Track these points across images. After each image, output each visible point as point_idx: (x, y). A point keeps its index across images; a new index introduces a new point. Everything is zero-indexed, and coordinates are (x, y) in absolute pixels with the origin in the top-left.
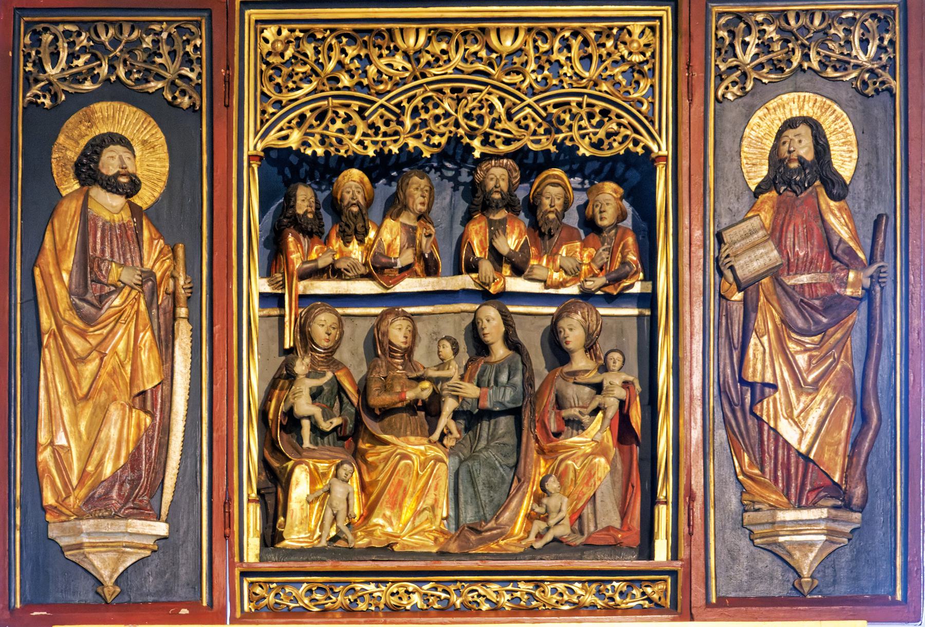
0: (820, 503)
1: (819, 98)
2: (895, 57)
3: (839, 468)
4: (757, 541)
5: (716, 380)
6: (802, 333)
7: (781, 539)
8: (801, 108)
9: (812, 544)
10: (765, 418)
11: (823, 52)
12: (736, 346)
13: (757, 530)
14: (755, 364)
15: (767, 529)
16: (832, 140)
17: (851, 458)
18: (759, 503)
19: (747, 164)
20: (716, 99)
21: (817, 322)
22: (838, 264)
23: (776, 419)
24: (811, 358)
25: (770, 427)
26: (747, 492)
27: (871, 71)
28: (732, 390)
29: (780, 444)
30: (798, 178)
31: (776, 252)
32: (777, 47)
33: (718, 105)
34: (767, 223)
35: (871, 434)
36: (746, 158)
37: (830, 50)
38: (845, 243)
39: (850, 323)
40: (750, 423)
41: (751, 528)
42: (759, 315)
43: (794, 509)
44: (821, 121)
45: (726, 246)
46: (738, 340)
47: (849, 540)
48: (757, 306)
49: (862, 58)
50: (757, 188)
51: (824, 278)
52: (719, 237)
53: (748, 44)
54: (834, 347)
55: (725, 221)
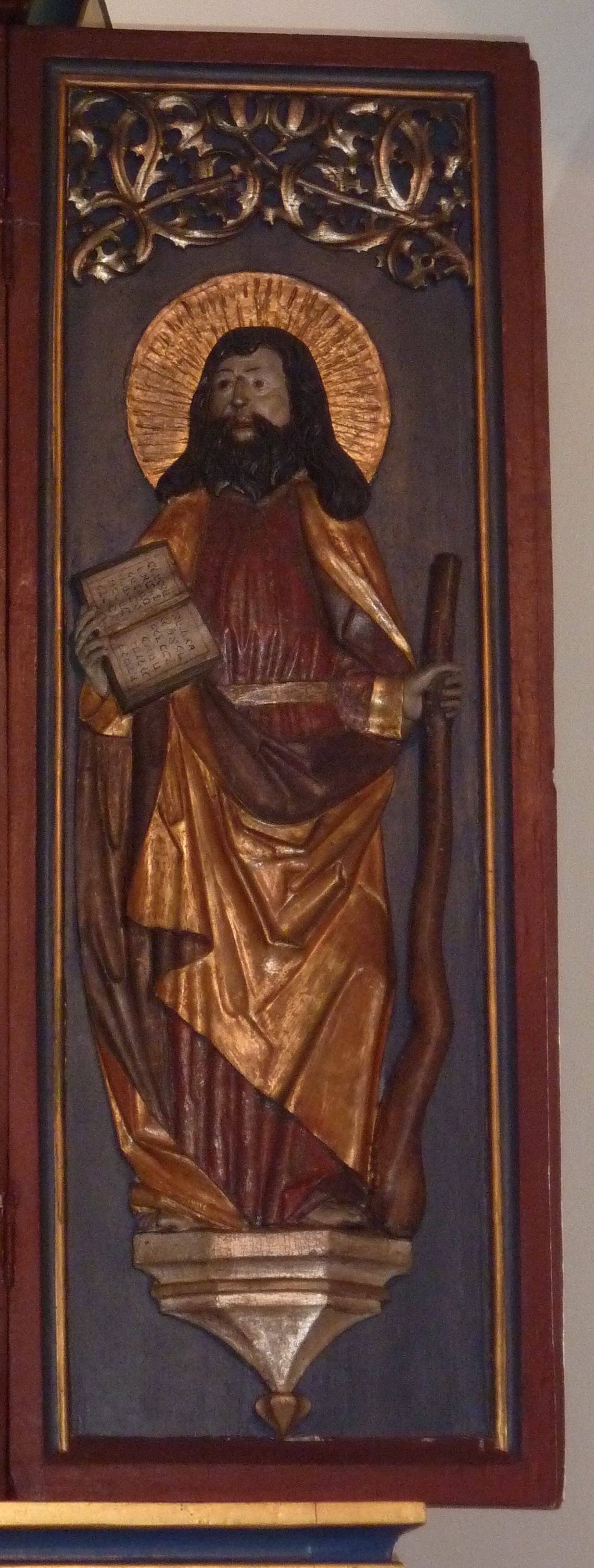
0: (315, 1216)
1: (302, 287)
2: (470, 207)
3: (356, 1133)
4: (169, 1303)
5: (69, 918)
6: (263, 814)
7: (224, 1300)
8: (262, 308)
9: (296, 1312)
10: (182, 1011)
11: (310, 188)
12: (116, 841)
13: (166, 1276)
14: (158, 887)
15: (189, 1275)
16: (332, 382)
17: (384, 1108)
18: (171, 1212)
19: (140, 426)
20: (68, 274)
21: (301, 795)
22: (347, 661)
23: (209, 1014)
24: (288, 875)
25: (194, 1034)
26: (144, 1186)
27: (416, 233)
28: (108, 943)
29: (219, 1074)
30: (255, 466)
31: (204, 630)
32: (206, 172)
33: (72, 290)
34: (186, 562)
35: (428, 1057)
36: (137, 412)
37: (326, 183)
38: (368, 614)
39: (379, 796)
40: (149, 1021)
41: (155, 1272)
42: (168, 772)
43: (253, 1229)
44: (306, 339)
45: (92, 613)
46: (121, 827)
47: (384, 1304)
48: (163, 752)
49: (398, 202)
50: (161, 481)
51: (315, 693)
52: (74, 585)
53: (141, 159)
54: (341, 851)
55: (89, 554)
